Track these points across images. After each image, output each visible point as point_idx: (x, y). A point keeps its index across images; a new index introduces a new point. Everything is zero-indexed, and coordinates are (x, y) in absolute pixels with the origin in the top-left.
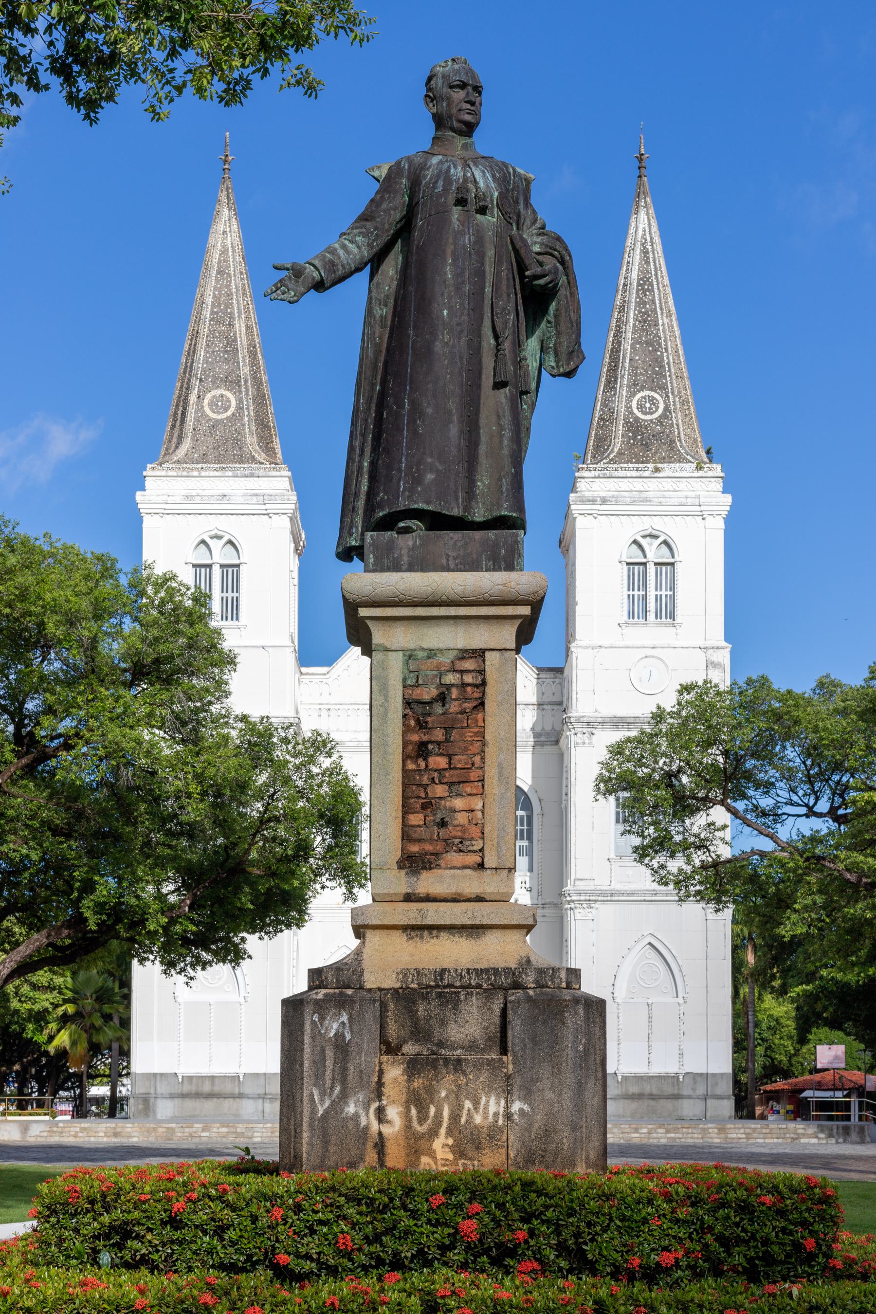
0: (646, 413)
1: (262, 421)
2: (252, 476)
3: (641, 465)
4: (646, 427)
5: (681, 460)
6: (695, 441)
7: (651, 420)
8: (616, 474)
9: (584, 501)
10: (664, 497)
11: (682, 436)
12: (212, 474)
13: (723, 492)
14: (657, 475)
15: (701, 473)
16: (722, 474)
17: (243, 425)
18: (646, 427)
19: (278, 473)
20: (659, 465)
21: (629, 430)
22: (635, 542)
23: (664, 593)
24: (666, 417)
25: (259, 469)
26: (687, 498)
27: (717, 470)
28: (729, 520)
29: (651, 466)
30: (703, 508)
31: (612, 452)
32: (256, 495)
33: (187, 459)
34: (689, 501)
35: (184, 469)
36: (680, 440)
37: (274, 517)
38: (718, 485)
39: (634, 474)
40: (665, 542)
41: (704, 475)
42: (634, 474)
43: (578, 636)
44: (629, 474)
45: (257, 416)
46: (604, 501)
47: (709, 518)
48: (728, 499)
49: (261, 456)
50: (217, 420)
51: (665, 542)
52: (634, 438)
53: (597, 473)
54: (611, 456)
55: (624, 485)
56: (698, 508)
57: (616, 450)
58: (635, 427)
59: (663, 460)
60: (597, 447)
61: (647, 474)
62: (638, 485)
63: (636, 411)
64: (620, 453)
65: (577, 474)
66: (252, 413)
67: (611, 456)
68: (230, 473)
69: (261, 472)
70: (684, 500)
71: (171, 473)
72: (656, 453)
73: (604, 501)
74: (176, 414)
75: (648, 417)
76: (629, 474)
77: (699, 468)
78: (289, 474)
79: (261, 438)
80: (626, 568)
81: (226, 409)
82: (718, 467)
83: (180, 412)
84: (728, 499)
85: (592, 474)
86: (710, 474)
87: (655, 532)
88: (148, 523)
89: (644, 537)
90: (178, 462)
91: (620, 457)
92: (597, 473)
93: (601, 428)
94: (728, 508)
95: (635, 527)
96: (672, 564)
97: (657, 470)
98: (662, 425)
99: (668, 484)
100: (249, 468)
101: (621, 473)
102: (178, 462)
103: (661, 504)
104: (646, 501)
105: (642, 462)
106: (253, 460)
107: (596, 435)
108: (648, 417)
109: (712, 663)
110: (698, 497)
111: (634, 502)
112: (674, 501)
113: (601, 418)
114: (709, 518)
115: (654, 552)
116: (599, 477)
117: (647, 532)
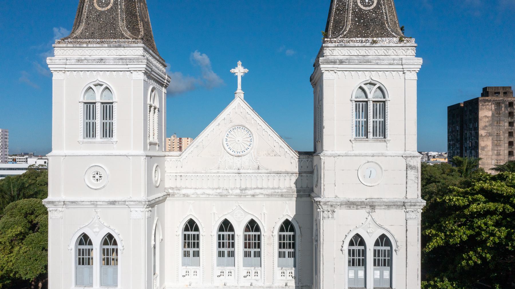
0: (365, 6)
1: (131, 12)
2: (120, 46)
3: (364, 39)
4: (366, 15)
5: (388, 35)
6: (395, 22)
7: (369, 10)
8: (348, 44)
9: (328, 62)
10: (379, 59)
11: (389, 20)
12: (95, 45)
13: (416, 56)
14: (374, 45)
15: (402, 44)
16: (416, 45)
17: (117, 14)
18: (366, 15)
19: (136, 45)
20: (375, 39)
21: (356, 17)
22: (361, 88)
23: (378, 120)
24: (379, 8)
25: (124, 42)
26: (394, 60)
27: (413, 42)
28: (420, 74)
29: (370, 39)
30: (404, 66)
31: (345, 30)
32: (122, 59)
33: (82, 36)
34: (395, 62)
35: (78, 42)
36: (387, 23)
37: (134, 73)
38: (412, 52)
39: (360, 44)
40: (379, 88)
41: (405, 45)
42: (360, 44)
43: (325, 148)
44: (357, 44)
45: (127, 8)
46: (341, 62)
47: (407, 73)
48: (420, 61)
49: (127, 34)
50: (101, 12)
51: (379, 88)
52: (359, 21)
53: (336, 44)
54: (345, 33)
55: (354, 52)
56: (401, 66)
57: (348, 29)
58: (359, 14)
59: (377, 36)
60: (335, 27)
61: (368, 44)
62: (363, 52)
63: (359, 4)
64: (350, 31)
65: (324, 45)
66: (123, 7)
67: (345, 33)
68: (106, 45)
69: (126, 44)
70: (392, 62)
71: (69, 45)
72: (373, 31)
73: (341, 62)
74: (80, 8)
75: (368, 8)
76: (357, 44)
77: (401, 41)
78: (143, 45)
79: (129, 23)
80: (354, 103)
81: (107, 5)
82: (413, 40)
83: (81, 7)
84: (420, 61)
85: (333, 45)
86: (408, 44)
87: (373, 82)
88: (56, 77)
89: (366, 84)
90: (76, 38)
91: (351, 34)
92: (336, 44)
93: (338, 15)
94: (420, 67)
95: (361, 78)
96: (384, 102)
97: (374, 42)
98: (376, 13)
99: (381, 51)
100: (118, 42)
101: (352, 44)
102: (76, 38)
103: (377, 64)
104: (368, 62)
105: (364, 37)
106: (123, 37)
107: (334, 19)
108: (368, 8)
109: (410, 166)
110: (401, 59)
111: (360, 63)
112: (386, 62)
113: (337, 9)
114: (407, 73)
115: (372, 94)
116: (338, 47)
117: (369, 82)
